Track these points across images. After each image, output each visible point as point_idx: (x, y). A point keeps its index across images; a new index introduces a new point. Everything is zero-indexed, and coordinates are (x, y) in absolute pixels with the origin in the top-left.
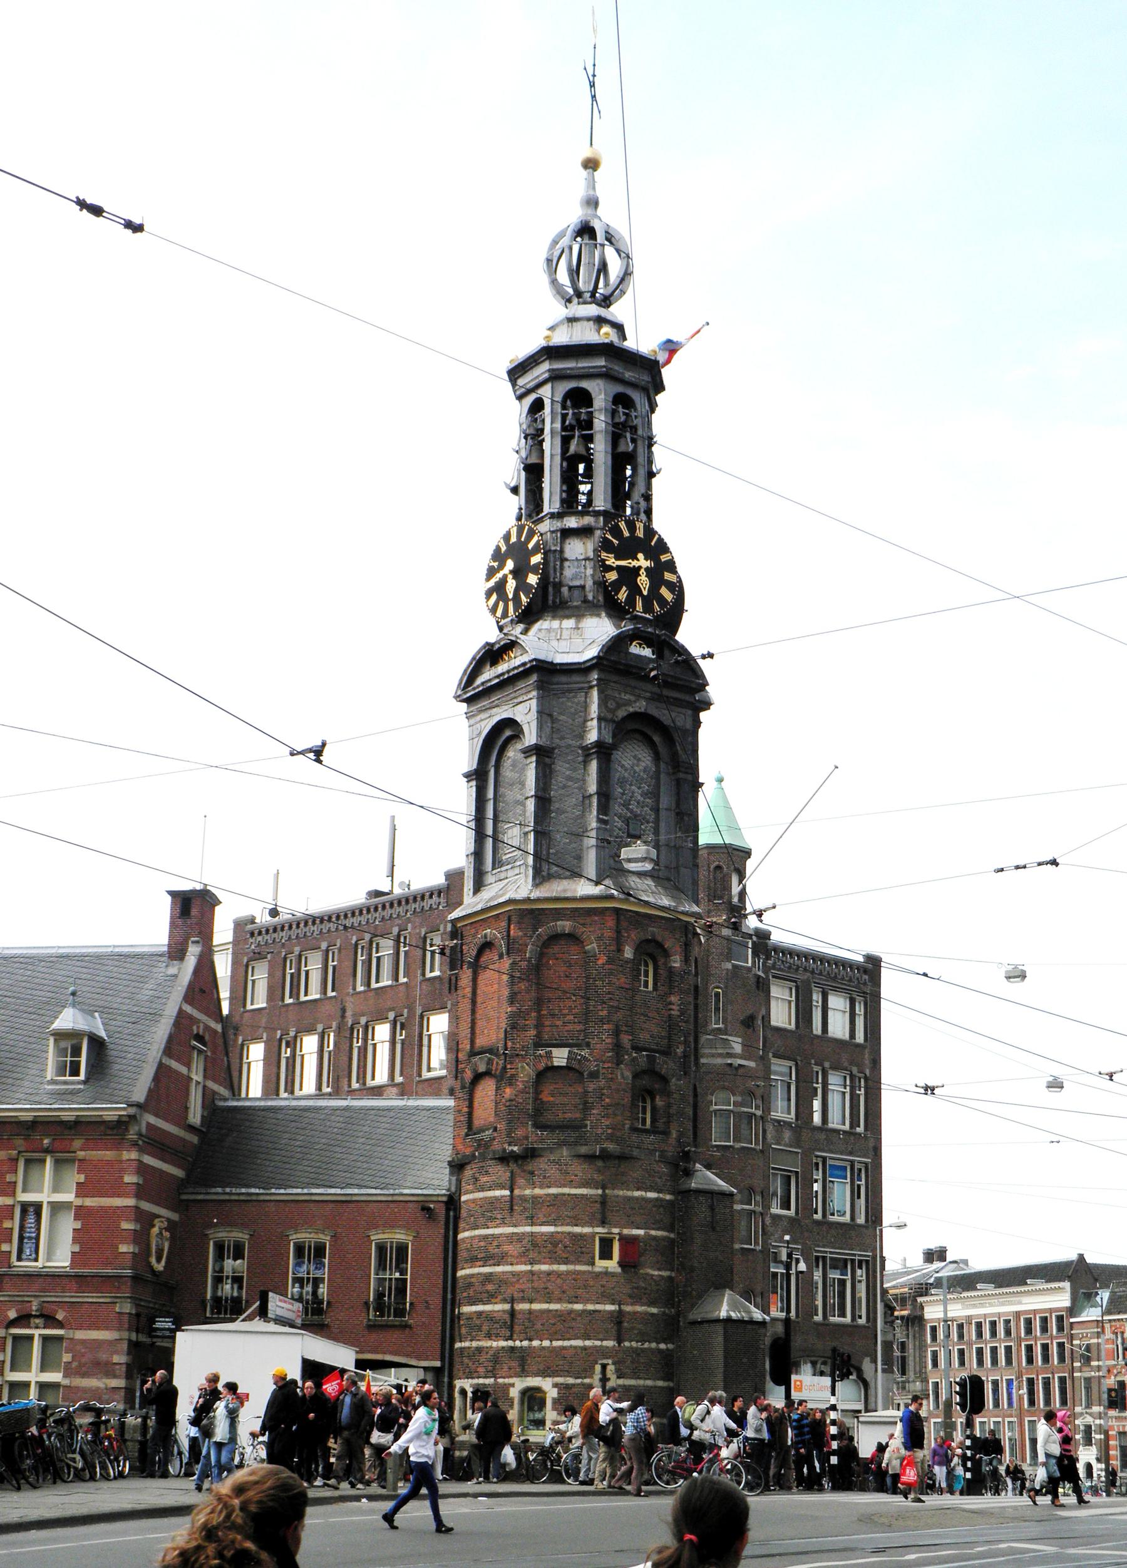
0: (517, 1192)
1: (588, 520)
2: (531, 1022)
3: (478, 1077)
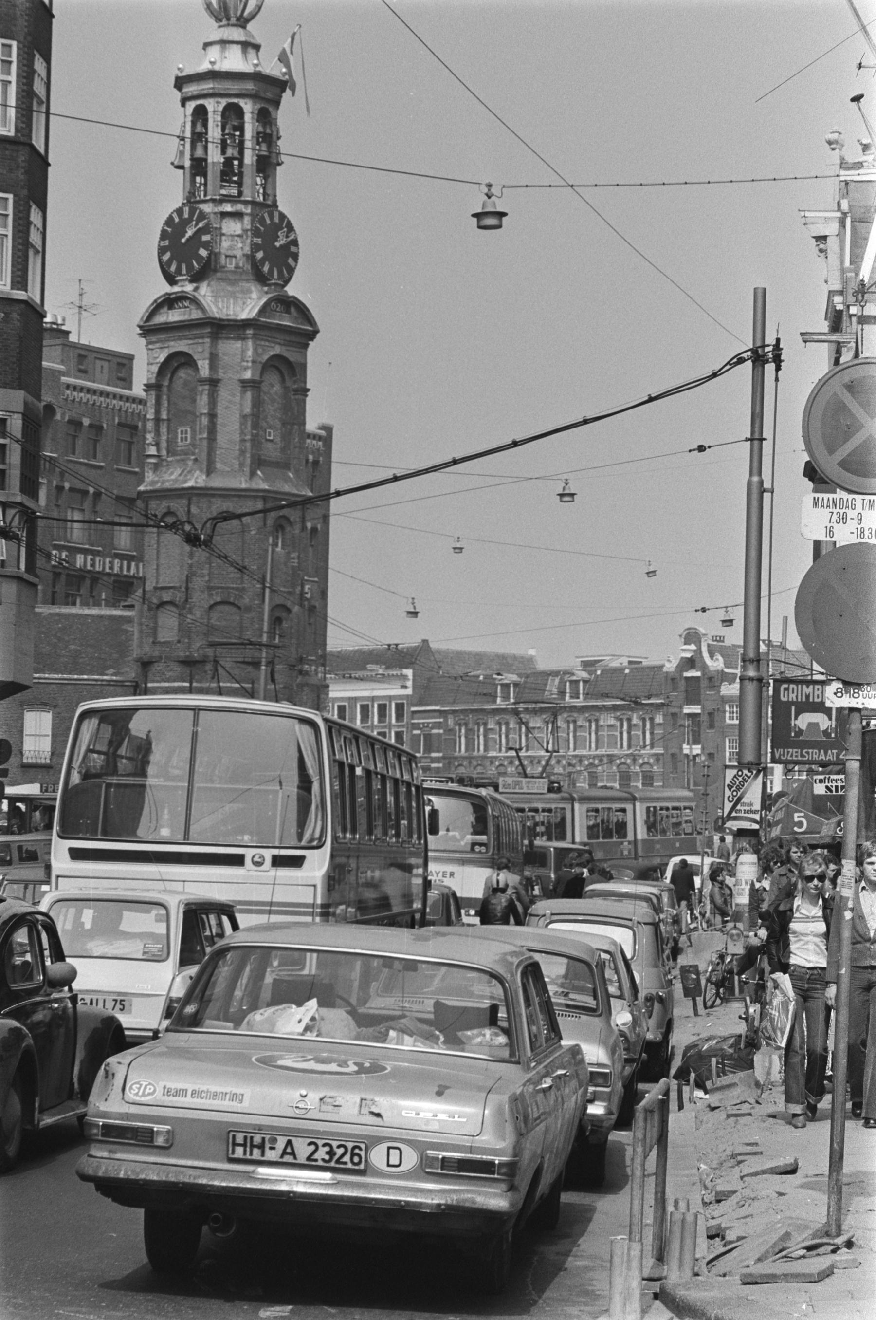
0: (195, 684)
1: (240, 207)
2: (206, 572)
3: (162, 604)
